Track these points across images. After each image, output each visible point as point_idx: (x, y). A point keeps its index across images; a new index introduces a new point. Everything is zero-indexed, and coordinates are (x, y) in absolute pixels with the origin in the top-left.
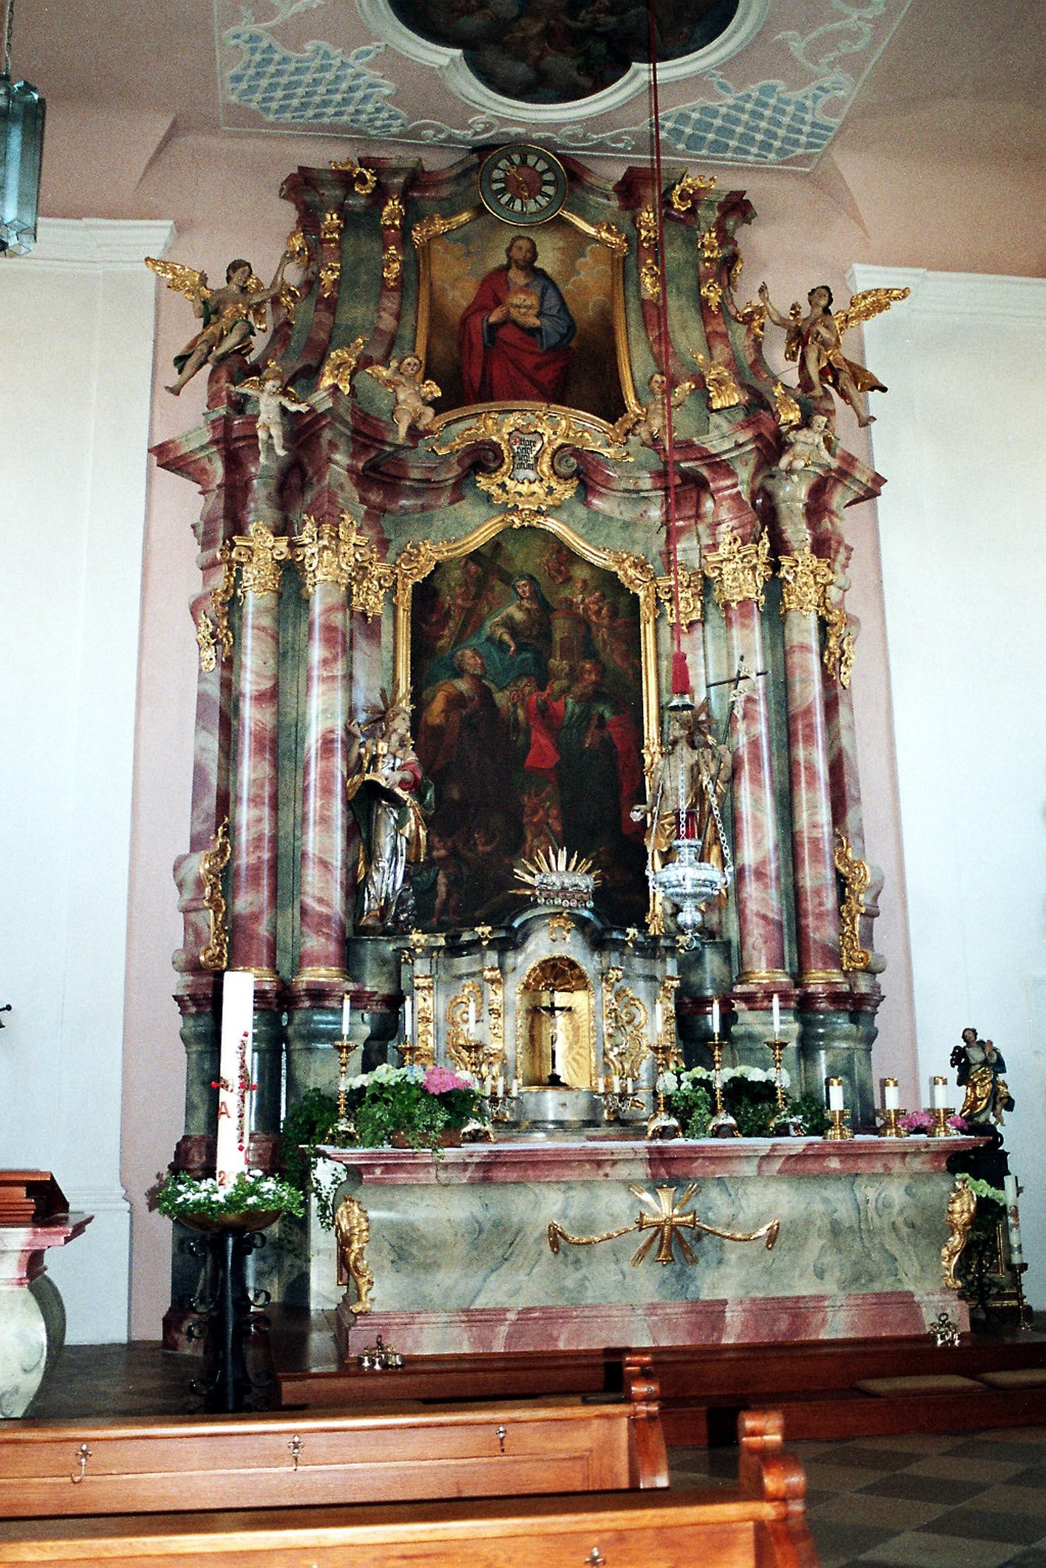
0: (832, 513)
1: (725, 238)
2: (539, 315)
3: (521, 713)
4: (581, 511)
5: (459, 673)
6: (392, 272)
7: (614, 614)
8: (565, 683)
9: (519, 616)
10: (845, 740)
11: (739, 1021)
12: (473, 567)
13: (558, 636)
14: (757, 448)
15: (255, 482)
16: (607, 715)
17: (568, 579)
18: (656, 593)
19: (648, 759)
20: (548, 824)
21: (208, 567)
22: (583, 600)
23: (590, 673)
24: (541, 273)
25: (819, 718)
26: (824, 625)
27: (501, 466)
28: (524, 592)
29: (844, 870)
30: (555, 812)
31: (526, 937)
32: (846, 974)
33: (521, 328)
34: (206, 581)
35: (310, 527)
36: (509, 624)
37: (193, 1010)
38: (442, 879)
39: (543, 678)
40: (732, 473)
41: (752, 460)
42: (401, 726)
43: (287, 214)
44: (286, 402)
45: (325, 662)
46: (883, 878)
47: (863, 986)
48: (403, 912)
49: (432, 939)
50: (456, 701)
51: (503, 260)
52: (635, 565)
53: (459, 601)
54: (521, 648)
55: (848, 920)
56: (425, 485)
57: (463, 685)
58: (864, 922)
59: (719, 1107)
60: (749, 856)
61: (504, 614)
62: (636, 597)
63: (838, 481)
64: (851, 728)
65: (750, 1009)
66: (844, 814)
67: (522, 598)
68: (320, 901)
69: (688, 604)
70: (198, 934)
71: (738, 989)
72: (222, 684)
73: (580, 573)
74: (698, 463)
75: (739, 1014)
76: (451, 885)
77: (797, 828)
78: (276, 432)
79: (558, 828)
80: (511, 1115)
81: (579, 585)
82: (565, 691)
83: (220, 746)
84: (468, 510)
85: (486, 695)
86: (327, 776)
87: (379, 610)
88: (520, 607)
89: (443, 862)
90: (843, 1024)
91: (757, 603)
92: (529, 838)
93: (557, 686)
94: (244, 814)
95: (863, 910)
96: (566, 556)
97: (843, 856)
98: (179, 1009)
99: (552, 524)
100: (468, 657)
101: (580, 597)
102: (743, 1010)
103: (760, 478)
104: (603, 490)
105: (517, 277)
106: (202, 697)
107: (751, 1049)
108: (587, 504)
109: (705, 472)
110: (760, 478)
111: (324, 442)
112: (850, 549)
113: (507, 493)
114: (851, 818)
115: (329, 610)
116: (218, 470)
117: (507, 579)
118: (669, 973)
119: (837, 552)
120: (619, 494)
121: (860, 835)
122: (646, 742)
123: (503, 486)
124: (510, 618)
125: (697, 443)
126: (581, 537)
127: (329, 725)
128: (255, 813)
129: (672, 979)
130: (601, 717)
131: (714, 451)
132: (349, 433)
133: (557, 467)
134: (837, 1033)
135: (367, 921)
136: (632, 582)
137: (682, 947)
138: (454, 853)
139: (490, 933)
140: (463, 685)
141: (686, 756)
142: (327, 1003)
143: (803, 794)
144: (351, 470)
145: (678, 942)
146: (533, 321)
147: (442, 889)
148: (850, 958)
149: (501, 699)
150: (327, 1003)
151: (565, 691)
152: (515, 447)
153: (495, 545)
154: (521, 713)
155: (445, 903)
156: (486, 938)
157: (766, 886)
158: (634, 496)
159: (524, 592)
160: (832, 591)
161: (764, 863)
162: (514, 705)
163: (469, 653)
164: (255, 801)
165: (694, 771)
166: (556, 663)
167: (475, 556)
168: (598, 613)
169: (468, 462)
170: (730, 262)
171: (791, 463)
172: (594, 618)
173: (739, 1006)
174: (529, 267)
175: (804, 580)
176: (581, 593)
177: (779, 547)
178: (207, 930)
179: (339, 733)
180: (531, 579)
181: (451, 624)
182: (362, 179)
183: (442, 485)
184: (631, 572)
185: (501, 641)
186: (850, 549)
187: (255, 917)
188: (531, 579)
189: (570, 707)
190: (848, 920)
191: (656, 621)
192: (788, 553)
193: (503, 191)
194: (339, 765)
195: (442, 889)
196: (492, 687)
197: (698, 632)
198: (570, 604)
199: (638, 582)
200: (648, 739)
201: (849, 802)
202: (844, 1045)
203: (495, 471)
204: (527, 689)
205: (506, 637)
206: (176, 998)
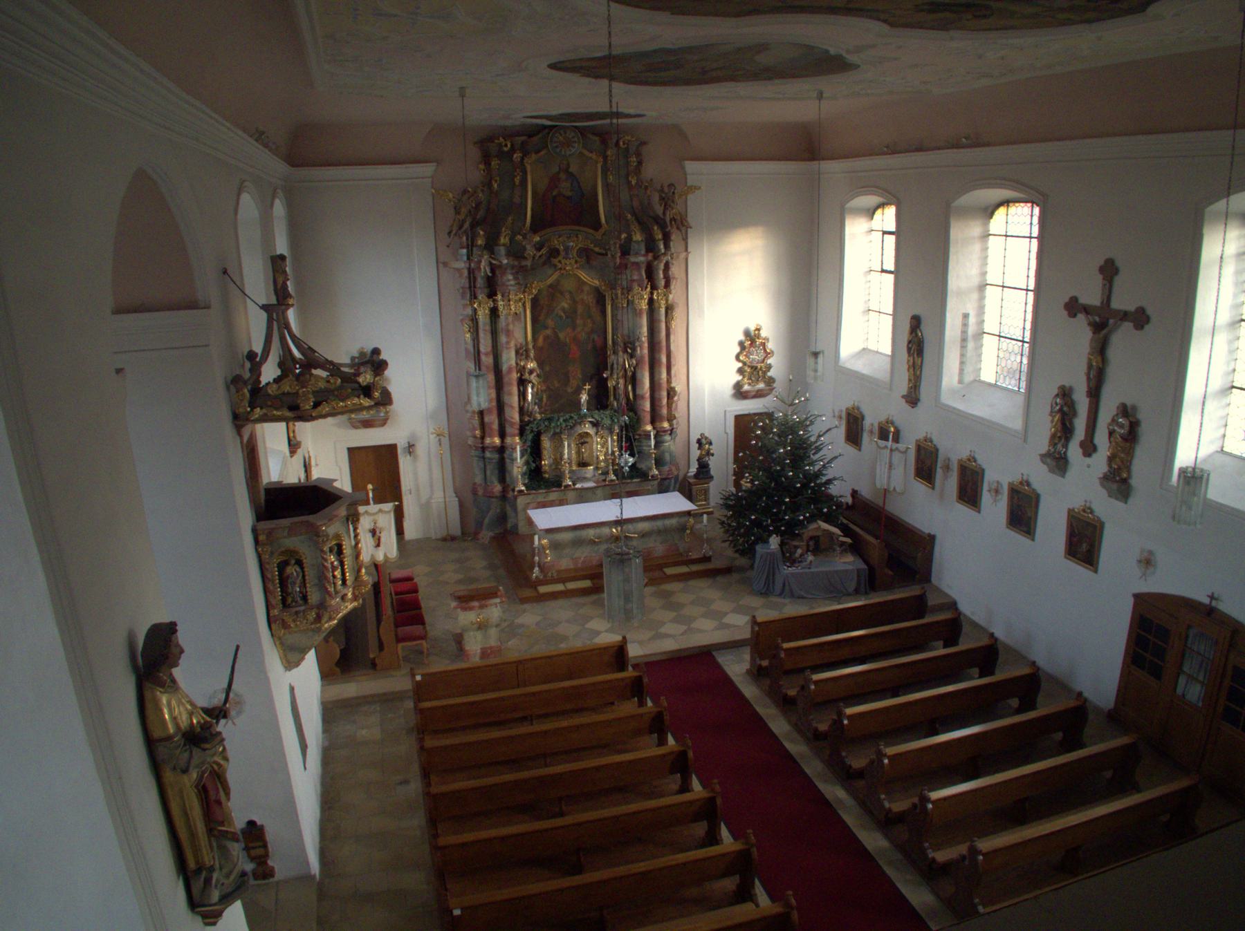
1: (638, 154)
2: (571, 191)
3: (568, 340)
5: (546, 328)
6: (517, 180)
7: (598, 302)
9: (566, 306)
10: (672, 347)
12: (550, 290)
17: (582, 291)
19: (609, 353)
21: (465, 306)
24: (571, 175)
25: (664, 343)
33: (564, 196)
35: (499, 297)
36: (563, 310)
38: (545, 396)
39: (574, 328)
42: (532, 354)
43: (474, 153)
50: (546, 338)
51: (558, 170)
54: (567, 317)
57: (548, 332)
73: (586, 288)
76: (549, 397)
78: (488, 270)
79: (580, 376)
85: (556, 334)
88: (567, 303)
89: (545, 391)
90: (667, 438)
92: (571, 381)
93: (579, 329)
96: (582, 283)
100: (550, 323)
105: (563, 176)
106: (466, 350)
113: (561, 263)
117: (562, 293)
121: (675, 376)
123: (560, 262)
130: (593, 339)
138: (548, 387)
140: (548, 332)
146: (569, 194)
147: (545, 399)
149: (561, 335)
153: (558, 281)
154: (568, 340)
155: (546, 404)
162: (566, 338)
163: (550, 321)
166: (579, 322)
167: (551, 286)
168: (592, 302)
170: (640, 163)
174: (567, 171)
177: (654, 288)
181: (544, 311)
182: (506, 145)
188: (570, 293)
193: (557, 147)
195: (545, 399)
198: (583, 300)
205: (562, 314)
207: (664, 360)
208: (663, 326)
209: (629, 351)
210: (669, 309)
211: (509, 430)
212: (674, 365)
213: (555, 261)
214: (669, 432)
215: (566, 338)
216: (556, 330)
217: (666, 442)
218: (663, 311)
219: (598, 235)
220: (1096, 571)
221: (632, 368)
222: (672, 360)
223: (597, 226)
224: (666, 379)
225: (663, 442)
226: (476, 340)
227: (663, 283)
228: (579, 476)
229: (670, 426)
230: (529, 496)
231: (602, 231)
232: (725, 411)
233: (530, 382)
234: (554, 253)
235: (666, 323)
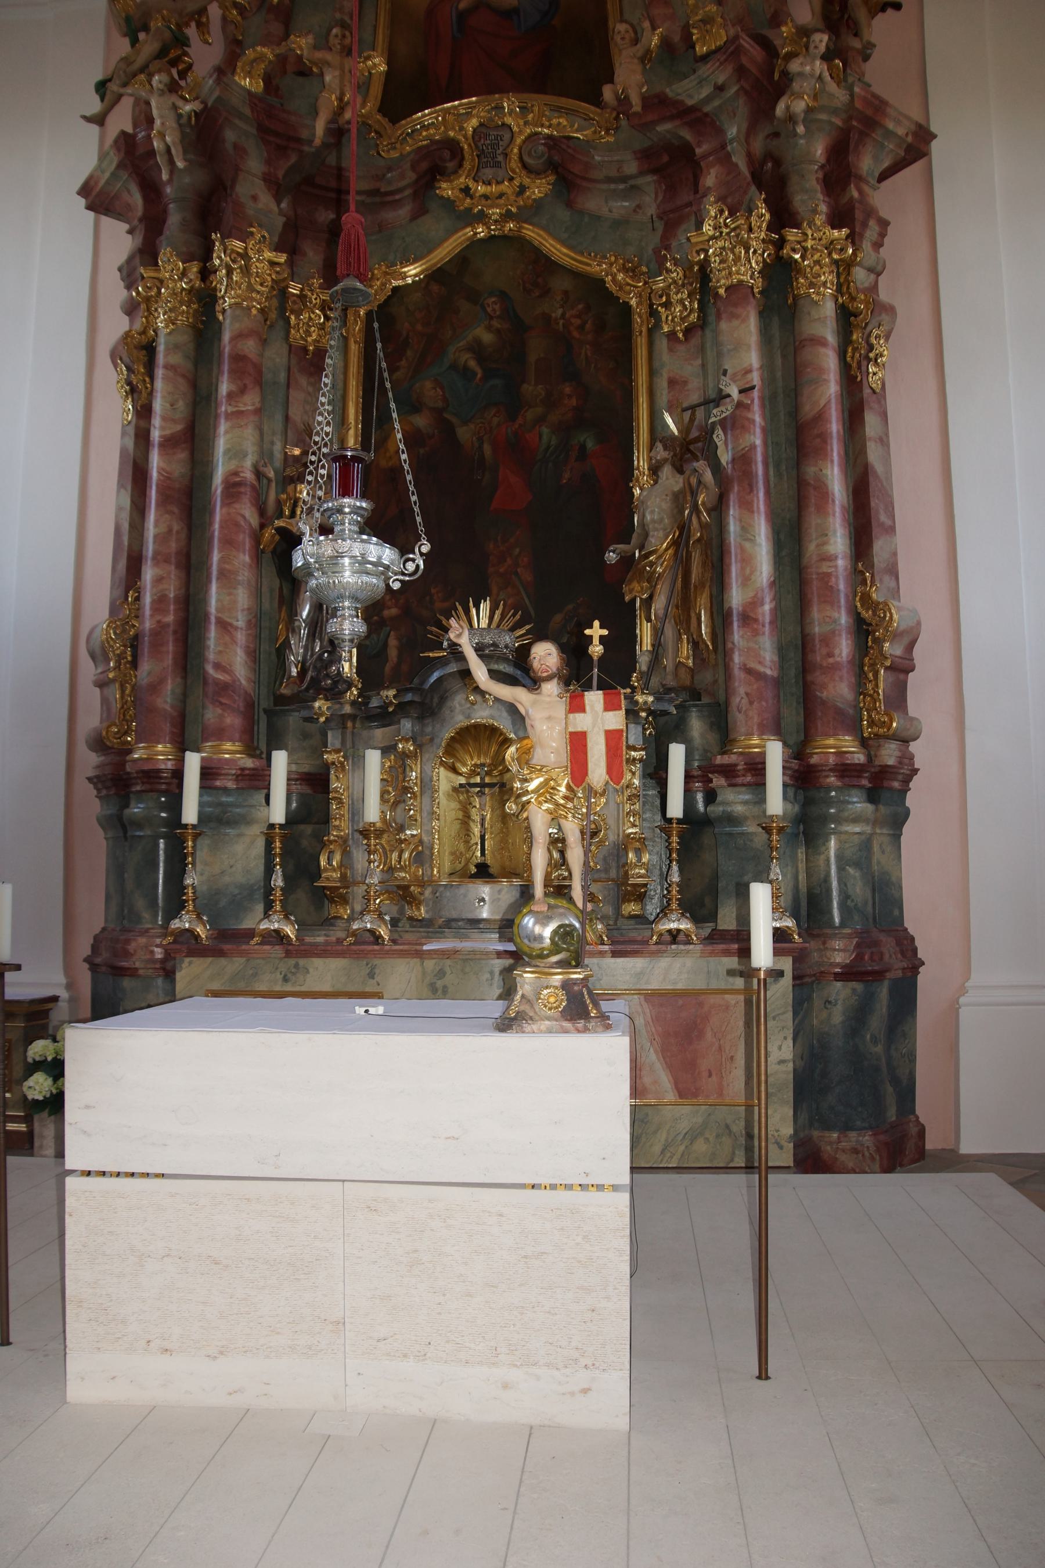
0: (860, 178)
3: (487, 449)
4: (563, 214)
8: (539, 410)
9: (487, 338)
11: (719, 799)
12: (435, 288)
13: (532, 358)
14: (742, 88)
15: (171, 206)
16: (590, 444)
17: (546, 292)
18: (650, 299)
19: (637, 491)
20: (516, 573)
22: (563, 315)
23: (570, 396)
25: (835, 426)
26: (846, 317)
27: (461, 166)
28: (494, 310)
29: (867, 615)
30: (526, 559)
31: (443, 700)
32: (864, 743)
34: (132, 322)
36: (477, 349)
37: (104, 792)
38: (393, 642)
40: (720, 131)
41: (742, 108)
44: (180, 103)
45: (230, 396)
46: (919, 623)
47: (889, 754)
48: (328, 676)
49: (337, 706)
52: (624, 269)
53: (419, 327)
55: (871, 675)
56: (377, 199)
58: (890, 680)
59: (674, 906)
60: (736, 597)
61: (470, 338)
62: (627, 306)
63: (863, 135)
64: (884, 441)
65: (731, 785)
66: (870, 545)
67: (491, 318)
68: (218, 666)
69: (684, 306)
70: (109, 710)
71: (719, 760)
72: (137, 436)
73: (560, 284)
74: (677, 123)
75: (718, 791)
77: (805, 561)
79: (528, 576)
80: (427, 912)
81: (559, 298)
82: (541, 420)
83: (132, 501)
84: (431, 225)
85: (448, 431)
86: (229, 524)
88: (489, 328)
90: (858, 804)
91: (752, 288)
93: (530, 415)
94: (149, 573)
95: (888, 663)
97: (866, 598)
98: (95, 792)
99: (530, 232)
100: (428, 390)
101: (560, 311)
102: (722, 787)
103: (761, 137)
104: (585, 184)
106: (123, 452)
107: (730, 834)
108: (569, 204)
109: (687, 135)
110: (761, 137)
111: (229, 146)
112: (884, 224)
114: (880, 548)
115: (238, 337)
116: (137, 199)
118: (631, 742)
120: (604, 186)
122: (636, 472)
123: (466, 191)
124: (478, 341)
125: (670, 94)
126: (563, 243)
127: (233, 465)
128: (159, 571)
129: (635, 749)
130: (583, 447)
131: (690, 102)
132: (254, 132)
133: (526, 158)
134: (846, 814)
135: (285, 691)
136: (621, 288)
137: (643, 710)
139: (395, 697)
141: (671, 480)
142: (218, 783)
143: (813, 520)
144: (268, 180)
145: (637, 702)
147: (393, 653)
148: (872, 723)
149: (464, 433)
150: (218, 783)
151: (541, 420)
152: (480, 144)
153: (462, 260)
154: (487, 449)
156: (391, 703)
157: (756, 633)
158: (622, 186)
159: (494, 310)
160: (860, 275)
161: (755, 603)
162: (481, 440)
163: (428, 384)
164: (159, 558)
165: (678, 499)
166: (530, 389)
168: (581, 328)
169: (424, 166)
171: (788, 108)
172: (576, 334)
175: (816, 257)
176: (562, 306)
178: (114, 702)
179: (249, 475)
180: (503, 295)
181: (409, 353)
183: (397, 197)
184: (620, 277)
185: (466, 368)
186: (884, 224)
187: (155, 688)
188: (503, 295)
189: (545, 438)
190: (871, 675)
191: (651, 332)
192: (798, 226)
194: (249, 514)
195: (393, 653)
196: (454, 420)
197: (695, 341)
199: (628, 288)
200: (638, 469)
201: (875, 530)
202: (857, 829)
203: (455, 172)
204: (496, 420)
205: (472, 364)
206: (89, 779)
208: (830, 361)
211: (211, 714)
213: (447, 190)
214: (865, 782)
215: (481, 440)
216: (446, 415)
217: (855, 820)
218: (829, 309)
225: (838, 819)
226: (144, 412)
228: (454, 915)
229: (870, 759)
230: (223, 961)
235: (845, 368)
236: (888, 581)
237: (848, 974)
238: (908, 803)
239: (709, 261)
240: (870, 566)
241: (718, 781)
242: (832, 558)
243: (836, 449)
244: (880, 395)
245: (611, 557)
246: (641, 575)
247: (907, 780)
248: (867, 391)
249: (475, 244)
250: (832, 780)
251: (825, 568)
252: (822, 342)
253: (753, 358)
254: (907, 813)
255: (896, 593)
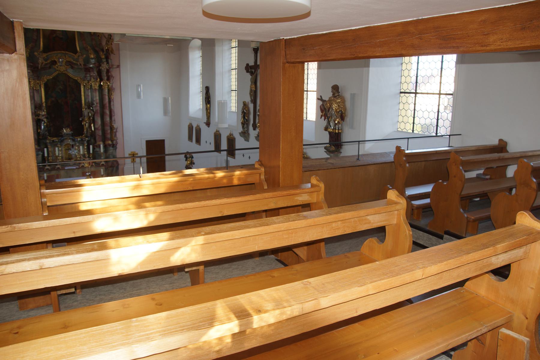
9: (61, 88)
10: (112, 107)
25: (108, 105)
29: (111, 126)
60: (96, 126)
64: (113, 105)
71: (95, 145)
87: (38, 88)
90: (111, 148)
97: (111, 125)
112: (113, 77)
114: (113, 119)
119: (111, 78)
121: (115, 120)
140: (53, 99)
167: (54, 78)
173: (95, 147)
186: (113, 77)
207: (107, 112)
208: (107, 97)
209: (91, 108)
210: (110, 90)
212: (114, 116)
213: (55, 67)
214: (112, 146)
217: (111, 150)
218: (107, 90)
219: (76, 56)
220: (200, 145)
221: (92, 116)
222: (112, 113)
223: (75, 52)
224: (109, 121)
227: (106, 78)
229: (112, 143)
231: (77, 55)
232: (141, 139)
233: (43, 120)
234: (54, 63)
236: (114, 122)
237: (111, 167)
238: (117, 146)
239: (89, 72)
240: (112, 121)
241: (95, 147)
242: (107, 121)
243: (108, 108)
244: (113, 99)
245: (81, 119)
246: (84, 121)
247: (117, 145)
248: (111, 99)
249: (59, 74)
250: (108, 146)
251: (107, 122)
252: (106, 95)
253: (98, 98)
254: (117, 148)
255: (115, 123)
